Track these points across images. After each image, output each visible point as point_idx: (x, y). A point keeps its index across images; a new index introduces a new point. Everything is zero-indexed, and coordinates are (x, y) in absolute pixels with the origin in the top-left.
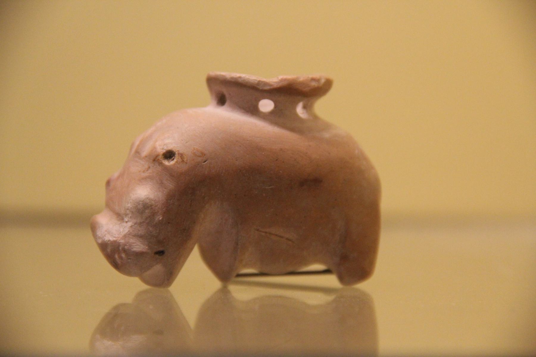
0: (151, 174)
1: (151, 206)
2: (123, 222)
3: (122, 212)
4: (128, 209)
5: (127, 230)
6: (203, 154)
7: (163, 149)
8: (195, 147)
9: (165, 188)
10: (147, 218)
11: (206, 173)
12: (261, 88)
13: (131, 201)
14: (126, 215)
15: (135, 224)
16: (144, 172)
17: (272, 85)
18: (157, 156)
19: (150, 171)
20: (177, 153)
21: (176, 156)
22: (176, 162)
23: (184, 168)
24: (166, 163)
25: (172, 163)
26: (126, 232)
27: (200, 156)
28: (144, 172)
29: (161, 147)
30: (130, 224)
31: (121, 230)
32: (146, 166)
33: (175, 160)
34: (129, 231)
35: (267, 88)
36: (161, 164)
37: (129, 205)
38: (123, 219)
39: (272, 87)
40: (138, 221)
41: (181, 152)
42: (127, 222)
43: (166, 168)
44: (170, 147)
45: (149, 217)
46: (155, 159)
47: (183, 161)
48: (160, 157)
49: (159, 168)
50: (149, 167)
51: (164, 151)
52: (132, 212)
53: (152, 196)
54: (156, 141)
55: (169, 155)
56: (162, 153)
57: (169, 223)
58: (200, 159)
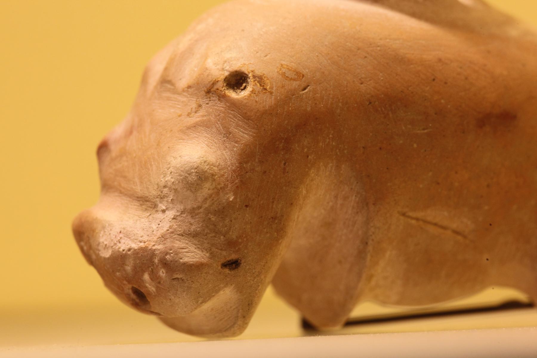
0: (205, 118)
2: (157, 211)
3: (153, 192)
4: (165, 187)
5: (165, 227)
6: (299, 75)
7: (223, 69)
8: (283, 63)
9: (236, 142)
11: (309, 109)
13: (171, 169)
14: (162, 198)
15: (182, 213)
16: (189, 115)
18: (215, 83)
20: (250, 75)
21: (251, 80)
23: (268, 101)
24: (233, 94)
26: (165, 229)
27: (294, 80)
28: (189, 115)
29: (219, 67)
30: (170, 214)
31: (155, 227)
32: (194, 106)
33: (249, 89)
34: (170, 227)
36: (222, 97)
37: (168, 178)
38: (155, 206)
40: (189, 207)
41: (258, 73)
42: (164, 211)
43: (234, 105)
44: (236, 66)
45: (211, 196)
47: (266, 89)
48: (221, 85)
49: (220, 106)
50: (200, 106)
51: (227, 74)
52: (176, 190)
53: (212, 158)
54: (205, 57)
55: (237, 80)
56: (223, 77)
57: (246, 206)
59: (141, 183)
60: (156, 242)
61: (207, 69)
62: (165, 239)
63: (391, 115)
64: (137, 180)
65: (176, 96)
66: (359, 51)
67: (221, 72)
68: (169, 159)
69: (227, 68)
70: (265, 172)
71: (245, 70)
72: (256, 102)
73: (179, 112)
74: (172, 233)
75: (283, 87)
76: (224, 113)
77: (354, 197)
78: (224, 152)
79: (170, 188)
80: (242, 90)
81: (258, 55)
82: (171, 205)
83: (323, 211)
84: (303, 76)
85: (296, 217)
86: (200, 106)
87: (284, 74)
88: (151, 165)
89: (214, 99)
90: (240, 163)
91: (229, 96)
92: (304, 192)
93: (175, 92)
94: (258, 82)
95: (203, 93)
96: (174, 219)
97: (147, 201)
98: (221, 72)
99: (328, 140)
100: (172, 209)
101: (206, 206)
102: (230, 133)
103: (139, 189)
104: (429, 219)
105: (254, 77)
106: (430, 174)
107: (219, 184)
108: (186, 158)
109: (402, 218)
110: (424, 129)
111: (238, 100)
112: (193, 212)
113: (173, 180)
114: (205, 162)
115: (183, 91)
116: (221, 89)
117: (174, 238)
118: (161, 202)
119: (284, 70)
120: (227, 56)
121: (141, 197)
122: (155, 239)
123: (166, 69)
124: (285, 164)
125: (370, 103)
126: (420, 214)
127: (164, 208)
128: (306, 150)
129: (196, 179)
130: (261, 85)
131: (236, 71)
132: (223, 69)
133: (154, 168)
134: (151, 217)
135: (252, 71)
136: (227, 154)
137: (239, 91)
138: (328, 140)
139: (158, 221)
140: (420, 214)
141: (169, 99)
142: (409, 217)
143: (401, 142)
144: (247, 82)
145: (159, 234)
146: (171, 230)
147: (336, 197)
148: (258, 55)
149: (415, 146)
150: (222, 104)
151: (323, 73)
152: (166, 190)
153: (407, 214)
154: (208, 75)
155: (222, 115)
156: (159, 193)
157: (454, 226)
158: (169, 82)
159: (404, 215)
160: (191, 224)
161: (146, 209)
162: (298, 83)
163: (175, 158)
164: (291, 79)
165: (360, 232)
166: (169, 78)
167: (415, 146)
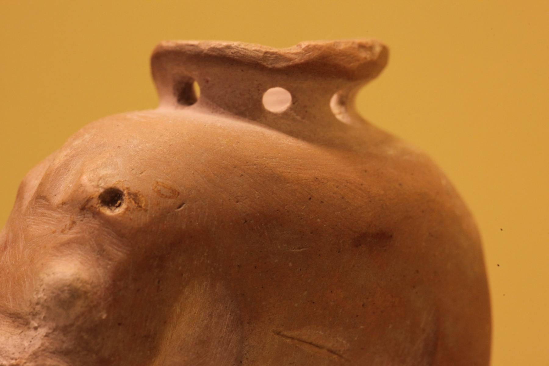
0: (79, 235)
1: (86, 293)
2: (29, 328)
3: (26, 309)
4: (37, 304)
5: (37, 344)
6: (175, 193)
7: (98, 186)
8: (159, 180)
9: (110, 260)
10: (78, 317)
11: (184, 227)
12: (270, 67)
13: (44, 286)
14: (34, 315)
15: (55, 330)
16: (63, 231)
17: (290, 60)
18: (89, 200)
19: (75, 229)
20: (125, 192)
21: (126, 197)
22: (127, 209)
23: (143, 219)
24: (107, 212)
25: (118, 211)
26: (37, 346)
27: (170, 197)
28: (63, 231)
29: (94, 183)
30: (42, 331)
31: (26, 344)
32: (68, 223)
33: (124, 206)
34: (42, 345)
35: (281, 65)
36: (97, 214)
37: (41, 295)
38: (27, 324)
39: (291, 63)
40: (61, 324)
41: (133, 190)
42: (36, 329)
43: (108, 222)
44: (112, 183)
45: (83, 314)
46: (83, 207)
47: (140, 207)
48: (95, 202)
49: (95, 223)
50: (74, 223)
51: (101, 190)
52: (48, 308)
53: (85, 275)
54: (81, 173)
55: (112, 197)
56: (97, 194)
57: (119, 324)
58: (170, 202)
59: (14, 299)
60: (27, 359)
61: (81, 185)
62: (37, 357)
63: (266, 234)
64: (9, 296)
65: (50, 212)
66: (235, 169)
67: (96, 189)
68: (42, 275)
69: (102, 185)
70: (138, 290)
71: (120, 187)
72: (131, 219)
73: (53, 228)
74: (44, 350)
75: (158, 204)
76: (98, 230)
77: (228, 316)
78: (98, 270)
79: (43, 306)
80: (117, 207)
81: (134, 172)
82: (43, 323)
83: (197, 329)
84: (179, 193)
85: (170, 335)
86: (74, 223)
87: (159, 192)
88: (24, 281)
89: (88, 215)
90: (114, 281)
91: (103, 213)
92: (178, 310)
93: (49, 207)
94: (133, 199)
95: (77, 209)
96: (46, 336)
97: (19, 318)
98: (96, 189)
99: (202, 258)
100: (44, 326)
101: (79, 323)
102: (104, 251)
103: (11, 306)
104: (304, 338)
105: (129, 194)
106: (306, 293)
107: (92, 302)
108: (59, 276)
109: (277, 337)
110: (299, 248)
111: (112, 217)
112: (65, 330)
113: (45, 297)
114: (78, 279)
115: (58, 207)
116: (95, 205)
117: (46, 356)
118: (33, 319)
119: (159, 188)
120: (103, 172)
121: (14, 314)
122: (27, 356)
123: (41, 185)
124: (159, 282)
125: (246, 221)
126: (295, 333)
127: (36, 325)
128: (180, 268)
129: (68, 297)
130: (135, 202)
131: (111, 188)
132: (98, 186)
133: (27, 284)
134: (23, 334)
135: (127, 188)
136: (100, 272)
137: (113, 208)
138: (202, 258)
139: (30, 338)
140: (295, 333)
141: (43, 215)
142: (284, 336)
143: (276, 261)
144: (122, 200)
145: (31, 351)
146: (42, 348)
147: (211, 315)
148: (134, 172)
149: (290, 265)
150: (96, 222)
151: (199, 191)
152: (38, 308)
153: (282, 333)
154: (83, 192)
155: (96, 232)
156: (32, 310)
157: (329, 345)
158: (44, 198)
159: (278, 334)
160: (63, 342)
161: (18, 326)
162: (173, 200)
163: (48, 275)
164: (166, 197)
165: (235, 351)
166: (44, 194)
167: (290, 265)
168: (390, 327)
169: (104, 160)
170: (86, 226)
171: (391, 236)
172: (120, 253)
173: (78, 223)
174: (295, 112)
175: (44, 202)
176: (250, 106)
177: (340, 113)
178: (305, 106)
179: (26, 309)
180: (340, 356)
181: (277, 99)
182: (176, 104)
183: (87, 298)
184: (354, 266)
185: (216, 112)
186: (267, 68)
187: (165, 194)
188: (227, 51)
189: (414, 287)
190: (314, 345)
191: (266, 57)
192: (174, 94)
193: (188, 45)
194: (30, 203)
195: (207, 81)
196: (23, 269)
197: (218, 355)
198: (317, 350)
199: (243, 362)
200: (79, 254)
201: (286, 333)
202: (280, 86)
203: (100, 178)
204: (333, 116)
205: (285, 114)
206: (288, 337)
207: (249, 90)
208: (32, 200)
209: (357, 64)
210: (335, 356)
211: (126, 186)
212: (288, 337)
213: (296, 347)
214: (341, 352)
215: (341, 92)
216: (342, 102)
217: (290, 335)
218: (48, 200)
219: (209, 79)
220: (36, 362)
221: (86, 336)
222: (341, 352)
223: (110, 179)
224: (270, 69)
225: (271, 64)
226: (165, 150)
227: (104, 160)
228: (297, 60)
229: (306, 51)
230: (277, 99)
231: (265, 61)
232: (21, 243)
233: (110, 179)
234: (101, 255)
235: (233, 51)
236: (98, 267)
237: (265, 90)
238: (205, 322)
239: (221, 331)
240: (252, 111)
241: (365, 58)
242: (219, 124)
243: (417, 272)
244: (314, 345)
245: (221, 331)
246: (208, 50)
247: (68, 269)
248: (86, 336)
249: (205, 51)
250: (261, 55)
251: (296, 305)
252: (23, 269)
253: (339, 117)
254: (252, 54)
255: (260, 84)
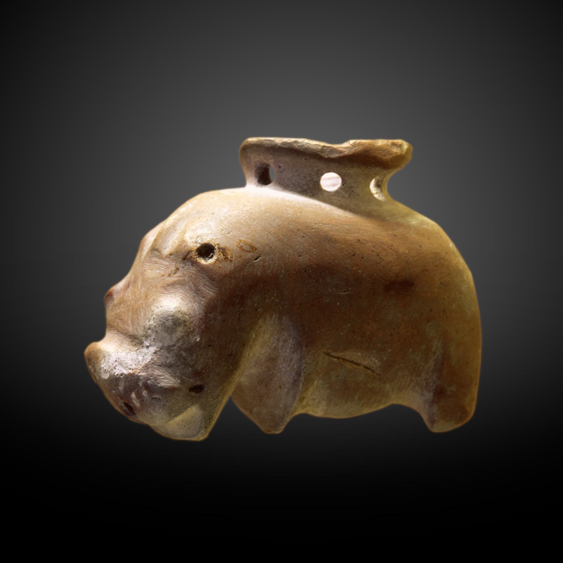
0: (181, 278)
1: (185, 322)
2: (143, 347)
3: (141, 332)
4: (149, 329)
5: (148, 358)
6: (253, 248)
7: (196, 242)
8: (242, 239)
9: (203, 297)
10: (179, 340)
11: (259, 274)
12: (326, 157)
13: (154, 316)
14: (147, 337)
15: (161, 349)
16: (169, 275)
17: (341, 152)
18: (190, 252)
19: (178, 274)
20: (216, 247)
21: (216, 251)
22: (217, 260)
23: (228, 267)
24: (203, 261)
25: (211, 261)
26: (148, 361)
27: (249, 252)
28: (169, 275)
29: (194, 240)
30: (152, 349)
31: (140, 358)
32: (173, 268)
33: (215, 257)
34: (152, 359)
35: (335, 155)
36: (195, 263)
37: (152, 322)
38: (141, 343)
39: (342, 155)
40: (166, 345)
41: (222, 246)
42: (148, 347)
43: (203, 269)
44: (206, 239)
45: (182, 337)
46: (185, 257)
47: (227, 258)
48: (193, 253)
49: (193, 270)
50: (178, 269)
51: (199, 245)
52: (157, 332)
53: (184, 309)
54: (184, 232)
55: (206, 250)
56: (196, 248)
57: (209, 346)
58: (249, 255)
59: (133, 325)
60: (141, 370)
61: (184, 241)
62: (148, 368)
63: (321, 281)
64: (130, 322)
65: (161, 261)
66: (299, 232)
67: (194, 244)
68: (153, 308)
69: (200, 241)
70: (224, 321)
71: (212, 243)
72: (220, 267)
73: (162, 273)
74: (153, 363)
75: (240, 257)
76: (195, 275)
77: (291, 341)
78: (194, 304)
79: (153, 330)
80: (210, 258)
81: (223, 232)
82: (153, 343)
83: (268, 350)
84: (256, 249)
85: (247, 354)
86: (178, 269)
87: (241, 247)
88: (140, 312)
89: (188, 264)
90: (206, 313)
91: (199, 263)
92: (254, 336)
93: (161, 257)
94: (222, 252)
95: (181, 259)
96: (155, 353)
97: (136, 339)
98: (194, 244)
99: (272, 298)
100: (154, 346)
101: (179, 344)
102: (199, 290)
103: (130, 329)
104: (347, 358)
105: (219, 248)
106: (349, 325)
107: (189, 328)
108: (166, 308)
109: (327, 357)
110: (345, 292)
111: (206, 265)
112: (169, 349)
113: (155, 324)
114: (179, 311)
115: (167, 257)
116: (193, 257)
117: (154, 368)
118: (146, 340)
119: (241, 244)
120: (199, 232)
121: (132, 336)
122: (141, 367)
123: (155, 240)
124: (239, 315)
125: (306, 271)
126: (340, 354)
127: (148, 344)
128: (256, 305)
129: (172, 324)
130: (223, 255)
131: (206, 244)
132: (196, 242)
133: (142, 314)
134: (138, 351)
135: (218, 244)
136: (196, 306)
137: (207, 259)
138: (272, 298)
139: (143, 354)
140: (340, 354)
141: (156, 263)
142: (332, 356)
143: (328, 301)
144: (214, 253)
145: (143, 364)
146: (152, 362)
147: (278, 340)
148: (223, 232)
149: (338, 304)
150: (194, 269)
151: (271, 247)
152: (149, 332)
153: (331, 354)
154: (185, 246)
155: (194, 276)
156: (145, 333)
157: (365, 363)
158: (157, 250)
159: (328, 354)
160: (167, 358)
161: (135, 345)
162: (252, 254)
163: (158, 308)
164: (247, 251)
165: (295, 366)
166: (157, 247)
167: (338, 304)
168: (410, 350)
169: (202, 223)
170: (188, 270)
171: (413, 284)
172: (211, 293)
173: (180, 269)
174: (344, 191)
175: (157, 253)
176: (311, 186)
177: (377, 193)
178: (352, 187)
179: (141, 332)
180: (373, 371)
181: (330, 181)
182: (257, 184)
183: (186, 325)
184: (385, 306)
185: (286, 190)
186: (324, 158)
187: (246, 249)
188: (295, 144)
189: (429, 322)
190: (354, 363)
191: (323, 150)
192: (256, 176)
193: (266, 140)
194: (147, 254)
195: (280, 167)
196: (139, 302)
197: (283, 369)
198: (356, 366)
199: (302, 375)
200: (181, 292)
201: (333, 354)
202: (334, 171)
203: (198, 236)
204: (372, 195)
205: (337, 192)
206: (335, 357)
207: (311, 174)
208: (149, 251)
209: (390, 157)
210: (369, 371)
211: (217, 243)
212: (335, 357)
213: (341, 364)
214: (374, 368)
215: (377, 177)
216: (378, 185)
217: (336, 355)
218: (159, 252)
219: (281, 165)
220: (147, 372)
221: (184, 354)
222: (374, 368)
223: (205, 237)
224: (327, 159)
225: (327, 155)
226: (247, 217)
227: (202, 223)
228: (346, 152)
229: (353, 146)
230: (330, 181)
231: (322, 153)
232: (140, 284)
233: (205, 237)
234: (197, 294)
235: (299, 145)
236: (194, 303)
237: (322, 174)
238: (274, 344)
239: (285, 351)
240: (312, 189)
241: (397, 153)
242: (287, 199)
243: (431, 310)
244: (354, 363)
245: (285, 351)
246: (281, 144)
247: (174, 302)
248: (184, 354)
249: (279, 145)
250: (320, 148)
251: (342, 334)
252: (139, 302)
253: (376, 196)
254: (313, 147)
255: (318, 170)
